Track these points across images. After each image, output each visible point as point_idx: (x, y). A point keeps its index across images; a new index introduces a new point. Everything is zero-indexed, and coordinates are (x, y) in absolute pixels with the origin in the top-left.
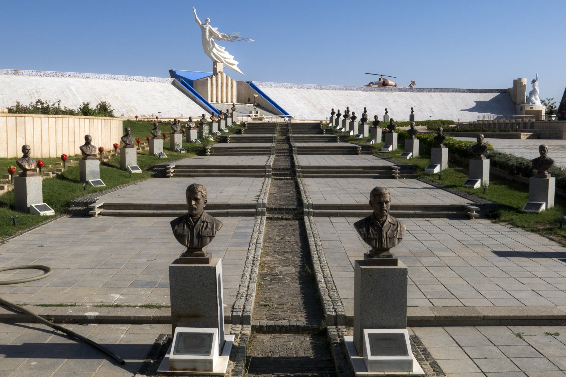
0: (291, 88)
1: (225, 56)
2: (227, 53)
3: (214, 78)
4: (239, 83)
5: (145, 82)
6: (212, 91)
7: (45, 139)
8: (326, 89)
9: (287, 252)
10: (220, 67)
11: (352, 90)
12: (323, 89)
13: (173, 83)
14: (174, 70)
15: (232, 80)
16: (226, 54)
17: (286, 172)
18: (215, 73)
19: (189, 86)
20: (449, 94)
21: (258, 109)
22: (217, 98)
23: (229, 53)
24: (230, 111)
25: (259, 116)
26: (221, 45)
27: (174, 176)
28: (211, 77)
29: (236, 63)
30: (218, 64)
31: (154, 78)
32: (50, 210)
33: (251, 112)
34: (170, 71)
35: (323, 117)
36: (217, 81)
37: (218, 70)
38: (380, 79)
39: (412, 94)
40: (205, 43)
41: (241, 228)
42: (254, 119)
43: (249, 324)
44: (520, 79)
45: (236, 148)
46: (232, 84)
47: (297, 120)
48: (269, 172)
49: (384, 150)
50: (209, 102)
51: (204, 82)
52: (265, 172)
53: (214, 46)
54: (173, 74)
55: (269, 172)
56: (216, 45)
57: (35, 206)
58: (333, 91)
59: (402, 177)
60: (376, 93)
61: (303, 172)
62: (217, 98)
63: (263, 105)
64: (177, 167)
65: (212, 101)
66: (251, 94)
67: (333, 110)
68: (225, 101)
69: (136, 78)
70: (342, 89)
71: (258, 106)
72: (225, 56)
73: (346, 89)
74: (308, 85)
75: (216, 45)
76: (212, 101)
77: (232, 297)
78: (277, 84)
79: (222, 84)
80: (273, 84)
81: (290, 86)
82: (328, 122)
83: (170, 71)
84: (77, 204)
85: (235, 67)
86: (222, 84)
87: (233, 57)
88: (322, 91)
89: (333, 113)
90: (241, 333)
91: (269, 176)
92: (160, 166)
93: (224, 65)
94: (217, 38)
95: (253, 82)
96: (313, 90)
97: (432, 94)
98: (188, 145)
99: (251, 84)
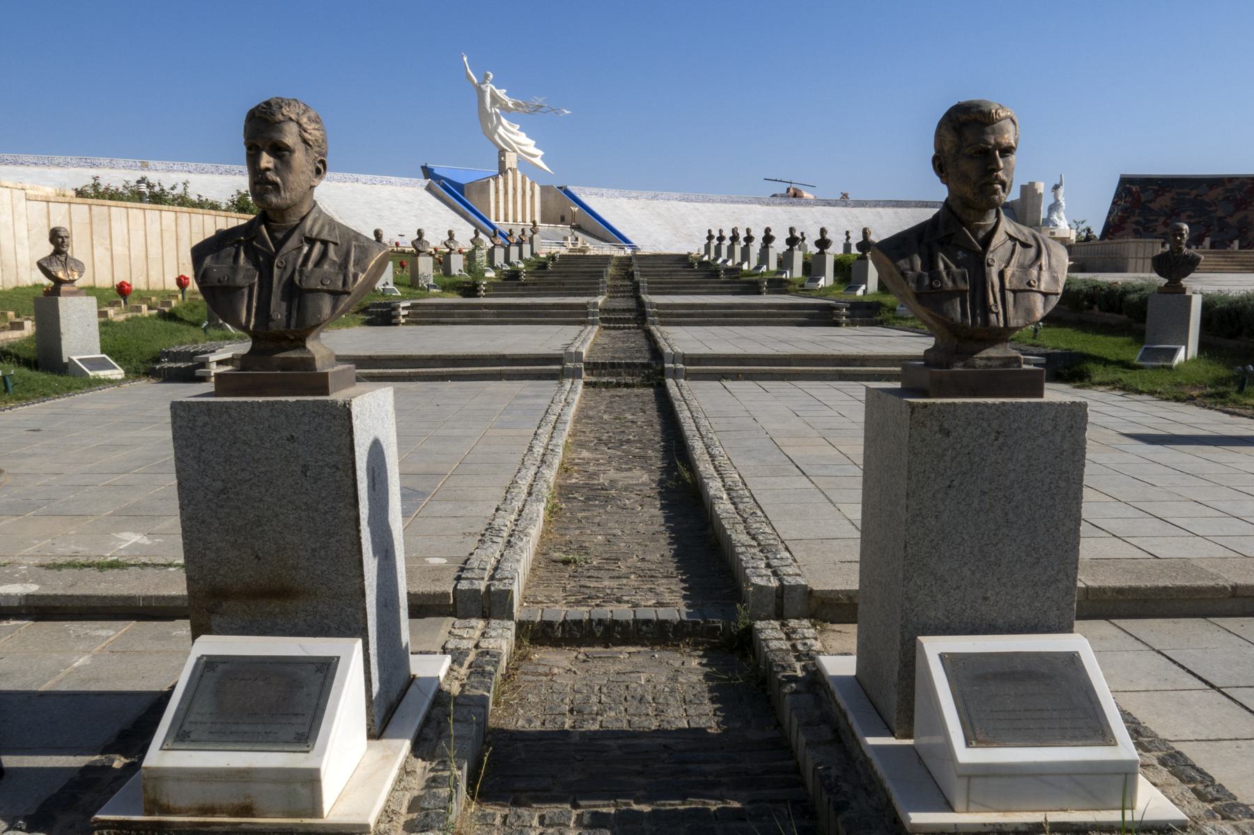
0: (637, 198)
1: (519, 140)
3: (501, 180)
4: (545, 190)
5: (379, 186)
6: (497, 202)
7: (154, 251)
8: (697, 201)
9: (628, 441)
10: (511, 160)
11: (743, 202)
13: (429, 189)
14: (429, 165)
16: (522, 138)
17: (627, 316)
18: (503, 170)
19: (456, 194)
20: (909, 210)
21: (577, 233)
22: (506, 215)
23: (528, 136)
24: (528, 233)
25: (579, 245)
26: (512, 120)
27: (407, 323)
28: (496, 178)
29: (540, 153)
31: (393, 179)
32: (114, 368)
33: (566, 239)
34: (423, 168)
35: (693, 246)
37: (508, 166)
38: (788, 190)
40: (484, 116)
41: (527, 397)
42: (571, 250)
43: (510, 617)
44: (1032, 184)
47: (647, 249)
48: (594, 314)
49: (808, 285)
50: (493, 221)
51: (483, 187)
52: (587, 315)
53: (500, 122)
54: (427, 172)
55: (594, 314)
56: (504, 121)
57: (80, 360)
59: (854, 324)
60: (783, 208)
61: (660, 315)
62: (506, 215)
63: (588, 227)
64: (413, 307)
65: (497, 220)
66: (565, 208)
67: (710, 231)
68: (519, 218)
69: (362, 177)
70: (725, 202)
71: (578, 228)
72: (519, 140)
73: (732, 202)
74: (665, 194)
75: (504, 121)
76: (497, 220)
77: (469, 539)
78: (611, 191)
79: (515, 189)
80: (604, 191)
81: (634, 194)
82: (702, 252)
83: (423, 168)
84: (175, 357)
85: (538, 161)
86: (515, 189)
88: (690, 205)
89: (710, 237)
90: (477, 646)
91: (593, 323)
92: (380, 305)
93: (519, 156)
94: (505, 108)
95: (569, 188)
96: (675, 203)
97: (880, 209)
98: (447, 280)
99: (567, 192)
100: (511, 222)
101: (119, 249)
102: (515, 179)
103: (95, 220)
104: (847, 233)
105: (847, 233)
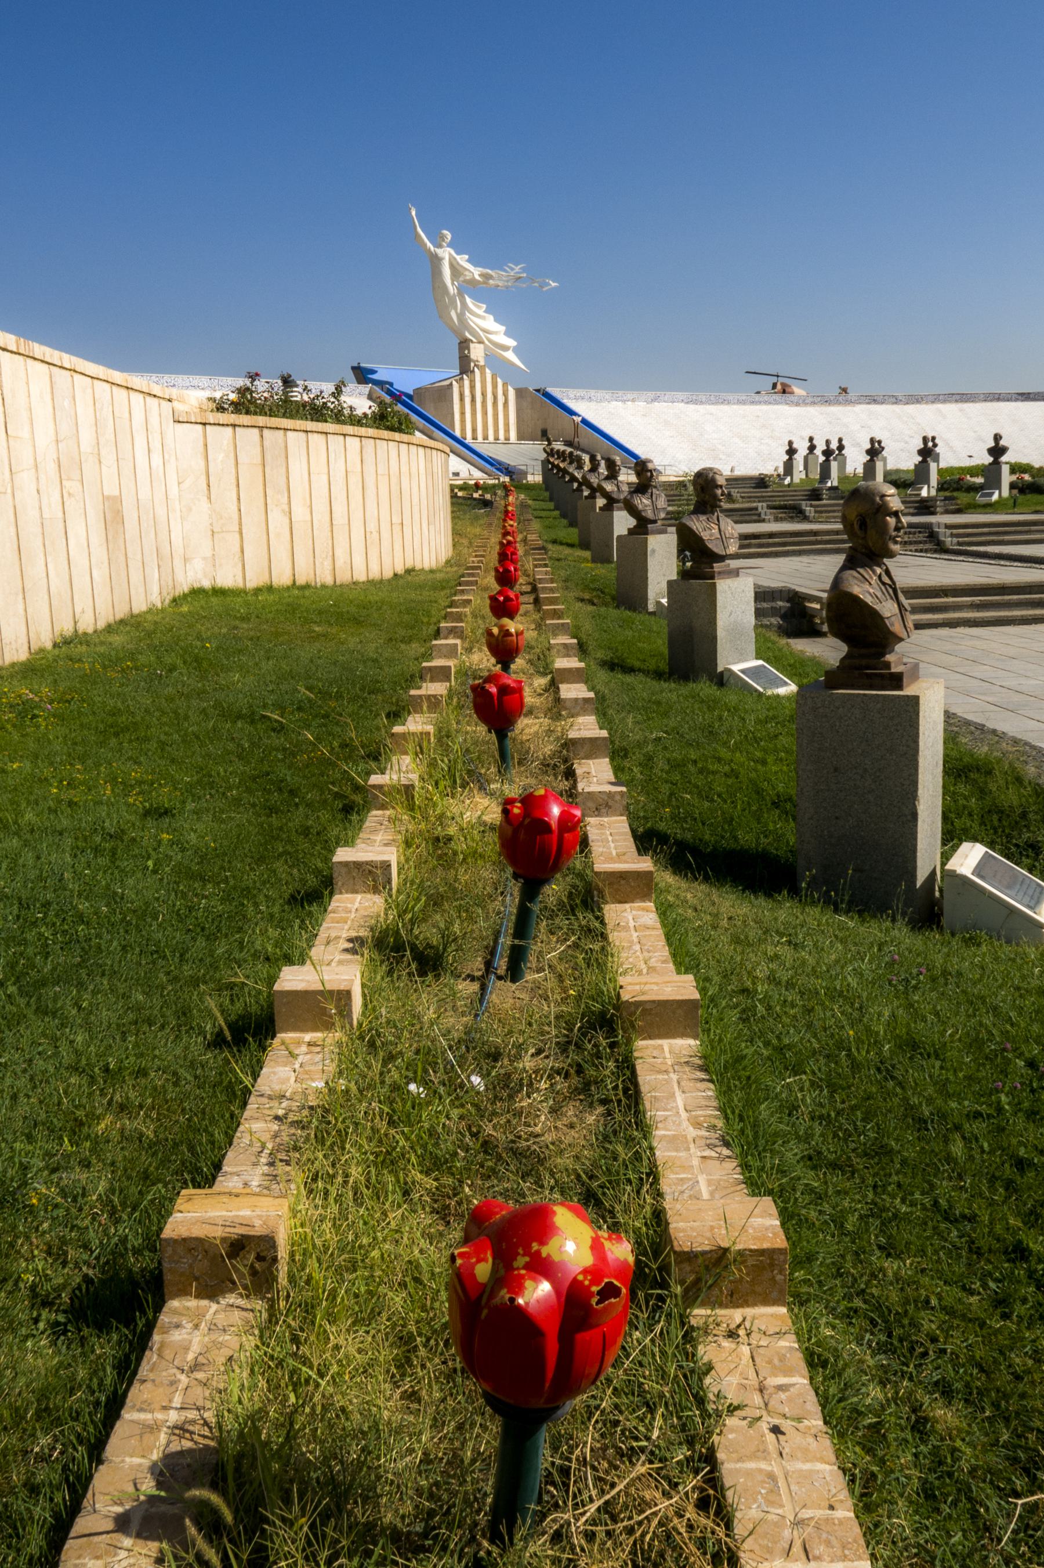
0: (633, 400)
1: (488, 327)
2: (491, 317)
3: (467, 383)
4: (520, 393)
7: (339, 510)
10: (477, 352)
12: (702, 403)
15: (505, 384)
16: (489, 323)
18: (465, 366)
22: (474, 430)
23: (496, 320)
29: (511, 343)
30: (472, 346)
34: (353, 368)
35: (771, 464)
36: (472, 387)
38: (774, 386)
39: (898, 408)
45: (771, 535)
46: (505, 394)
51: (442, 394)
58: (725, 408)
62: (474, 430)
65: (475, 438)
67: (790, 443)
76: (475, 438)
78: (600, 394)
79: (484, 395)
80: (592, 393)
81: (630, 396)
82: (781, 471)
83: (353, 368)
85: (510, 356)
86: (484, 395)
87: (503, 328)
89: (791, 451)
95: (549, 390)
97: (940, 406)
99: (547, 395)
100: (491, 438)
101: (300, 512)
102: (483, 379)
103: (268, 457)
104: (811, 439)
105: (811, 439)
